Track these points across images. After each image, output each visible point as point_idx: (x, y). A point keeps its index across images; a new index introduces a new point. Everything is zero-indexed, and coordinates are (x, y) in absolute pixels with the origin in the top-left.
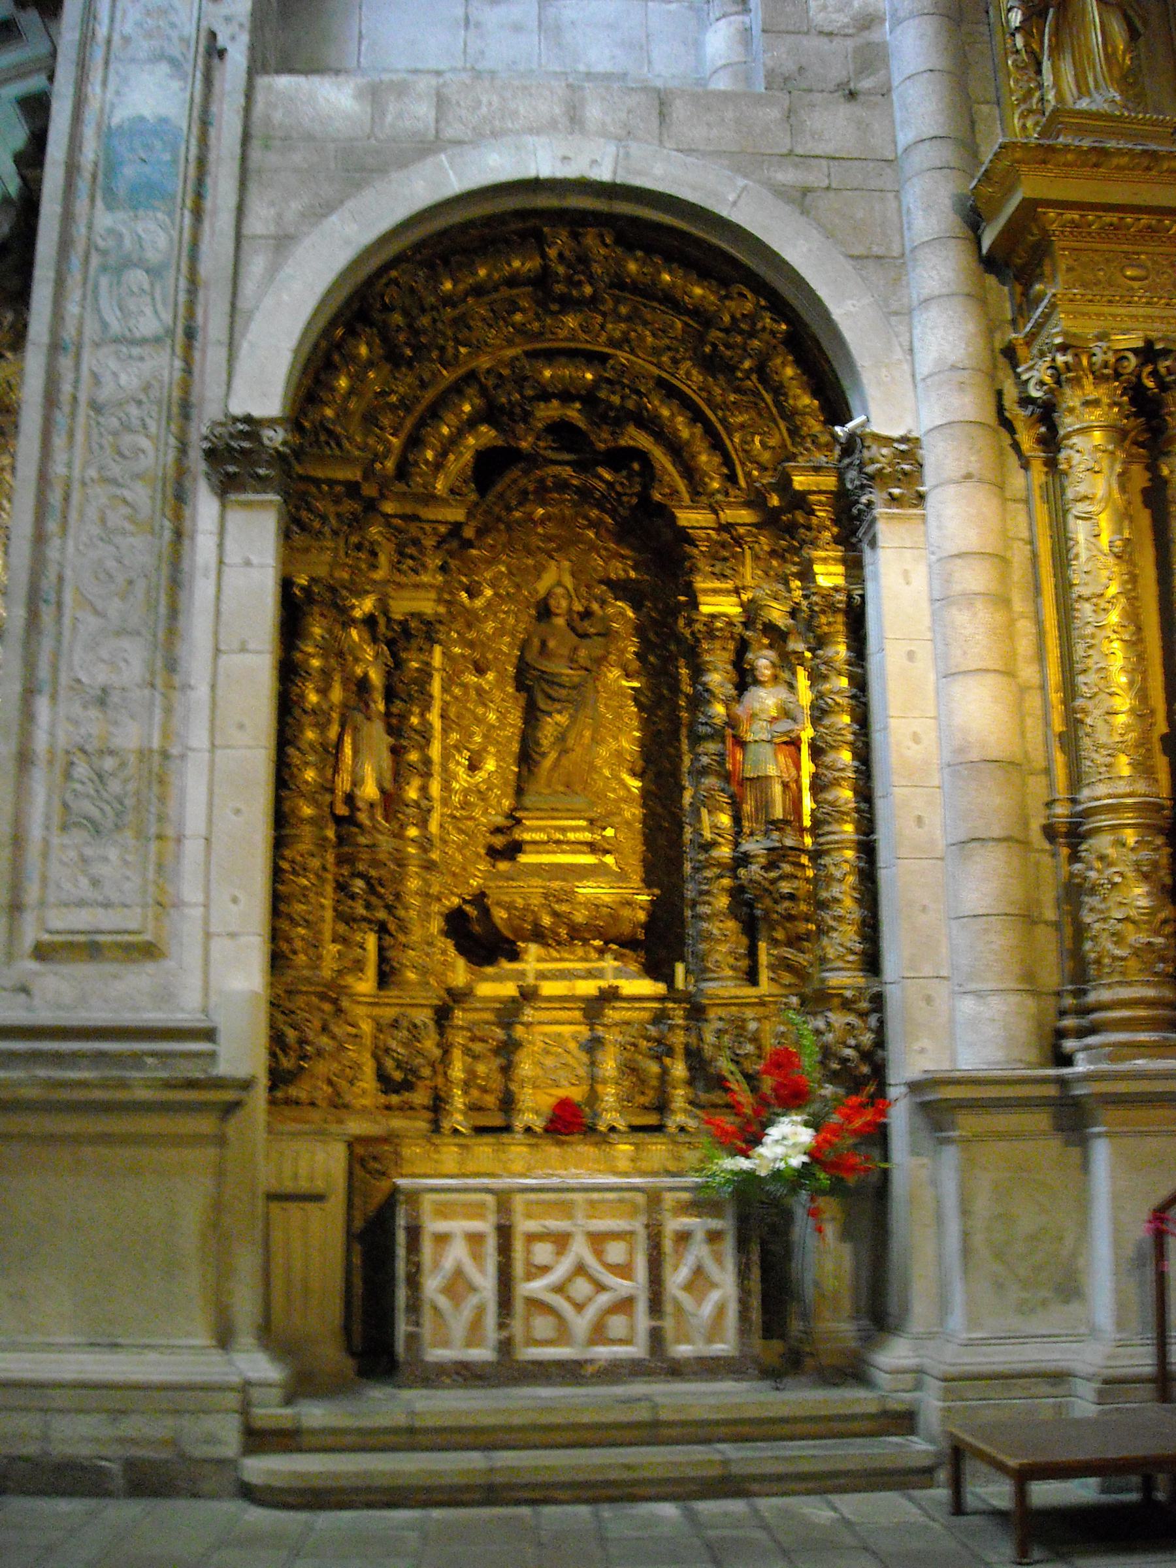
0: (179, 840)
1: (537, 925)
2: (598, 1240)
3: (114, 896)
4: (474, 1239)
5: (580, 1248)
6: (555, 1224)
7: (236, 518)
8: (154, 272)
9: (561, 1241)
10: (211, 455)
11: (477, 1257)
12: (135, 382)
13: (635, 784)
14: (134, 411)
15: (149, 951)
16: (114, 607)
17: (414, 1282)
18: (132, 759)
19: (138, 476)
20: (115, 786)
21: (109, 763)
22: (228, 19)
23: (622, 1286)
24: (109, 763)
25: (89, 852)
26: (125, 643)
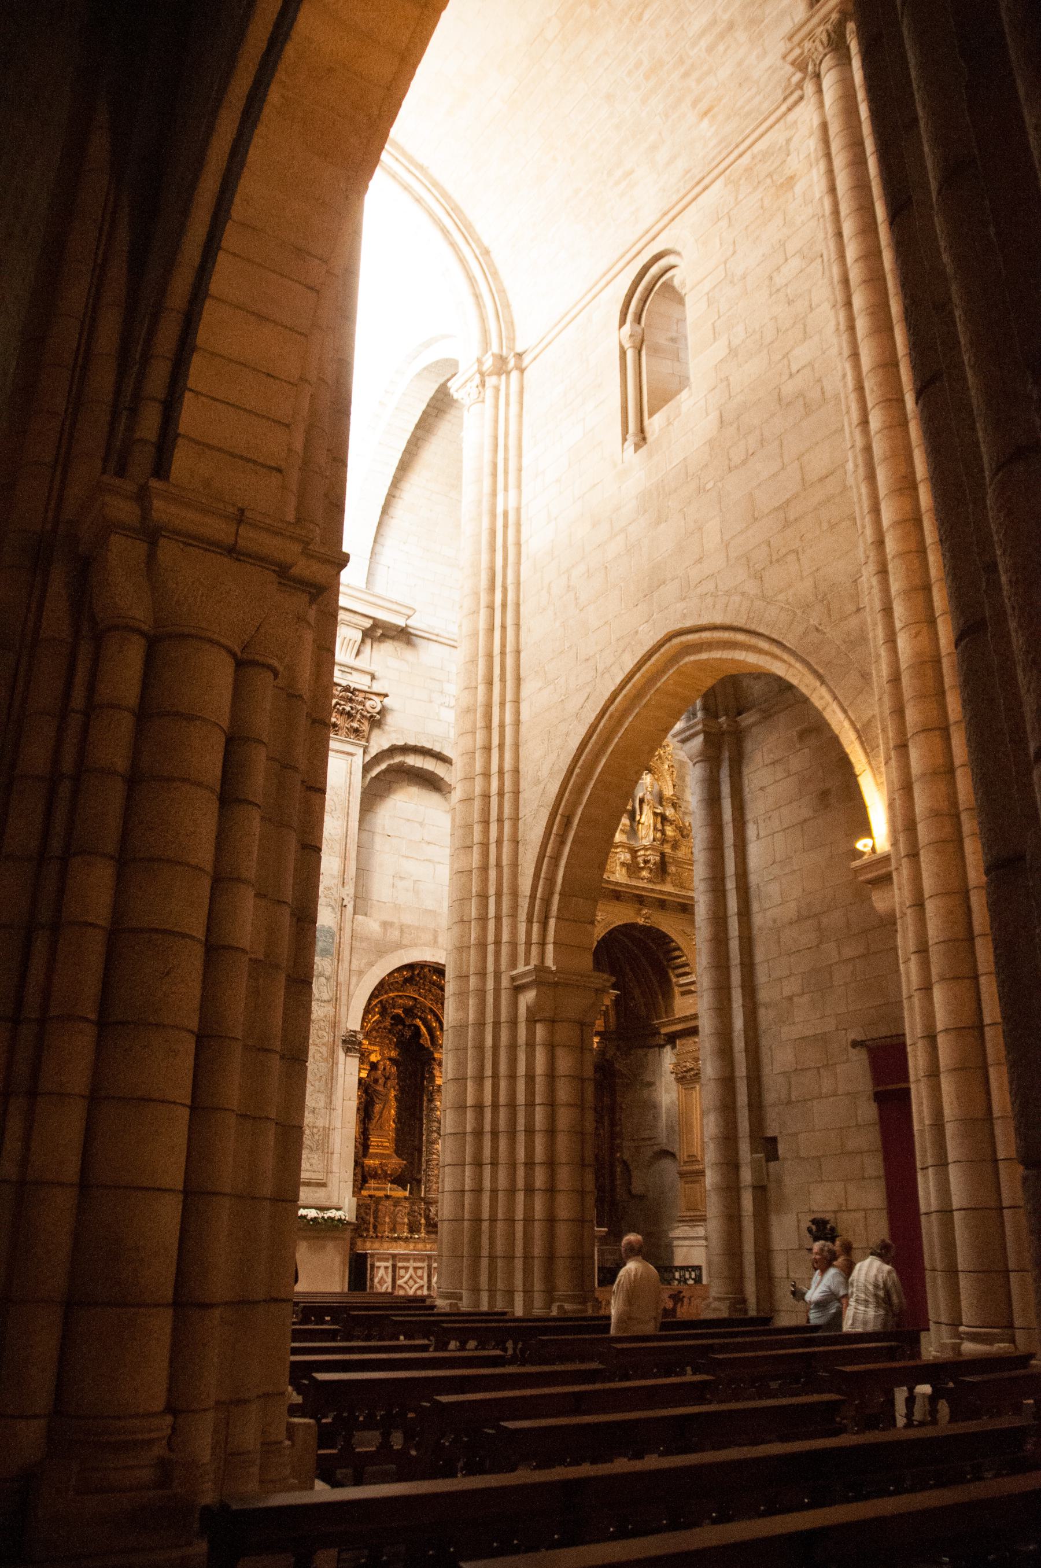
0: (332, 1153)
1: (376, 1173)
2: (416, 1269)
3: (316, 1169)
4: (386, 1268)
5: (411, 1271)
6: (405, 1264)
7: (348, 1059)
8: (328, 979)
9: (407, 1268)
10: (344, 1041)
11: (387, 1273)
12: (322, 1015)
13: (394, 1125)
14: (322, 1023)
15: (324, 1185)
16: (317, 1083)
17: (372, 1280)
18: (321, 1129)
19: (323, 1044)
20: (316, 1137)
21: (315, 1130)
22: (348, 895)
23: (421, 1282)
24: (315, 1130)
25: (310, 1156)
26: (320, 1095)
